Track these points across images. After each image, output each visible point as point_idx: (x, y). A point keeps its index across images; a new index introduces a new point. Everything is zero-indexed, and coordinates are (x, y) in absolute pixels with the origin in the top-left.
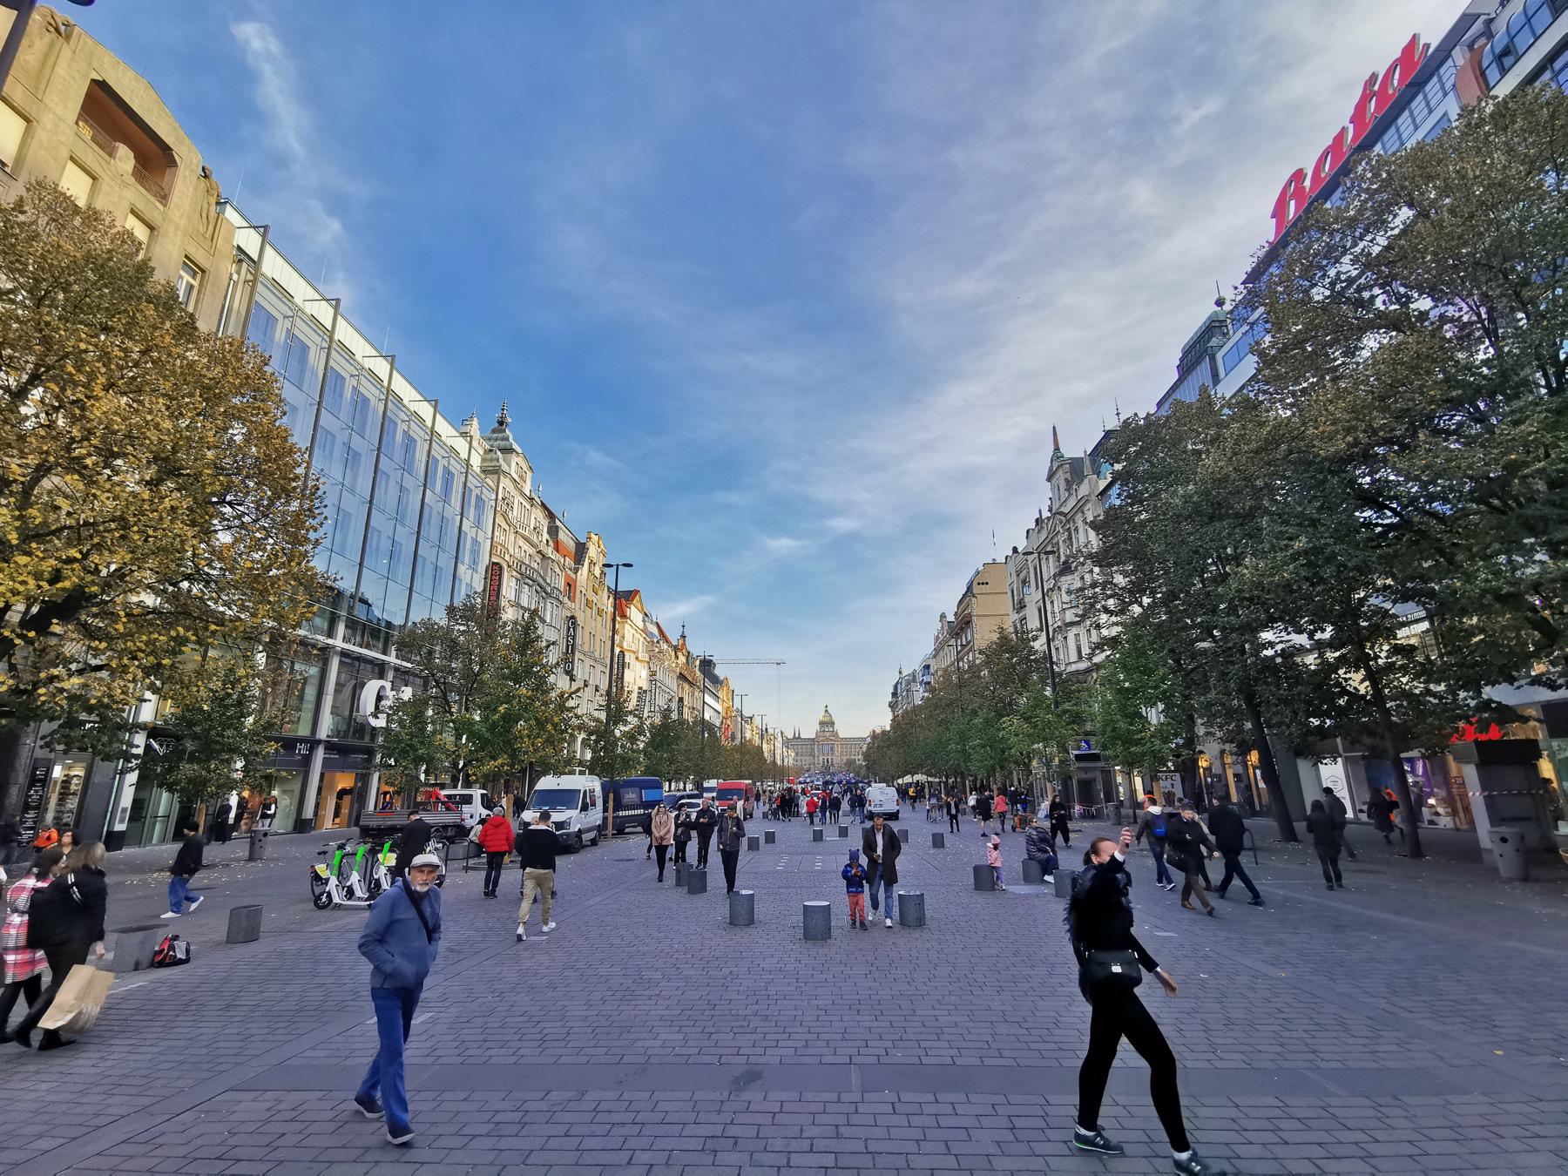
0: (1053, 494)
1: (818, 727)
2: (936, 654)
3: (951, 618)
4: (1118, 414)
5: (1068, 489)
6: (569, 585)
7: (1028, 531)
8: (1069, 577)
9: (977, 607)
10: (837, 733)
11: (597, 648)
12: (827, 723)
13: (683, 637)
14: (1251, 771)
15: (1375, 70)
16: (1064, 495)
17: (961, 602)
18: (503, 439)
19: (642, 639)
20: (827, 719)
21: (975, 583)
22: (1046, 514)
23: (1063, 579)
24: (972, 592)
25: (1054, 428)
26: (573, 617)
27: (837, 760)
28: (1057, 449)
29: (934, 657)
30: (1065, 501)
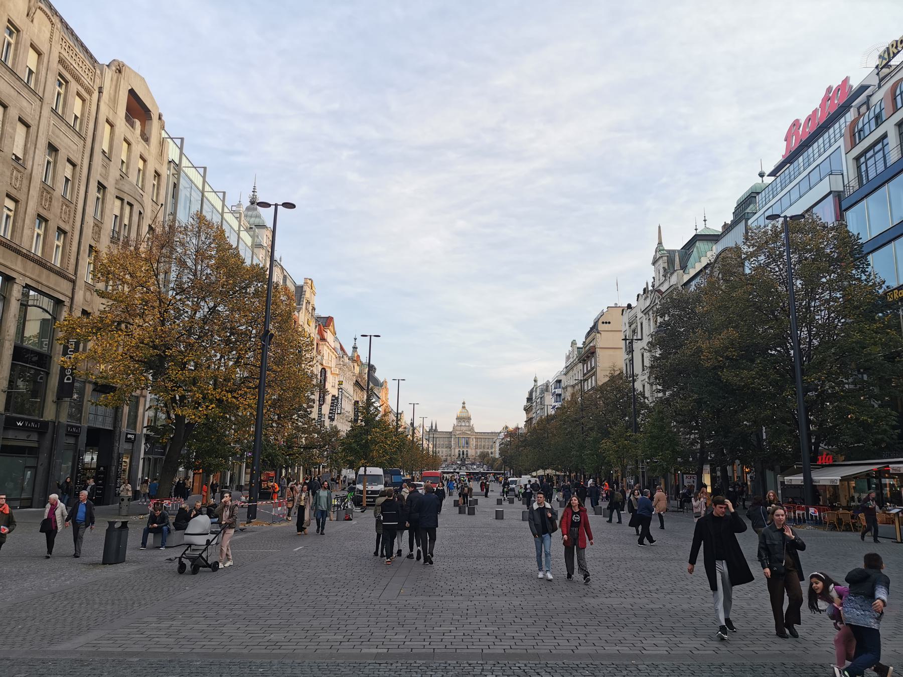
0: (656, 275)
1: (455, 422)
2: (569, 369)
3: (580, 345)
4: (705, 221)
5: (665, 276)
7: (638, 296)
9: (601, 341)
10: (472, 429)
12: (464, 419)
13: (355, 348)
14: (745, 475)
15: (831, 84)
16: (662, 279)
17: (589, 334)
18: (256, 217)
19: (334, 356)
20: (464, 415)
21: (600, 322)
22: (650, 288)
24: (597, 330)
25: (659, 227)
27: (471, 452)
28: (660, 243)
29: (565, 374)
30: (662, 283)
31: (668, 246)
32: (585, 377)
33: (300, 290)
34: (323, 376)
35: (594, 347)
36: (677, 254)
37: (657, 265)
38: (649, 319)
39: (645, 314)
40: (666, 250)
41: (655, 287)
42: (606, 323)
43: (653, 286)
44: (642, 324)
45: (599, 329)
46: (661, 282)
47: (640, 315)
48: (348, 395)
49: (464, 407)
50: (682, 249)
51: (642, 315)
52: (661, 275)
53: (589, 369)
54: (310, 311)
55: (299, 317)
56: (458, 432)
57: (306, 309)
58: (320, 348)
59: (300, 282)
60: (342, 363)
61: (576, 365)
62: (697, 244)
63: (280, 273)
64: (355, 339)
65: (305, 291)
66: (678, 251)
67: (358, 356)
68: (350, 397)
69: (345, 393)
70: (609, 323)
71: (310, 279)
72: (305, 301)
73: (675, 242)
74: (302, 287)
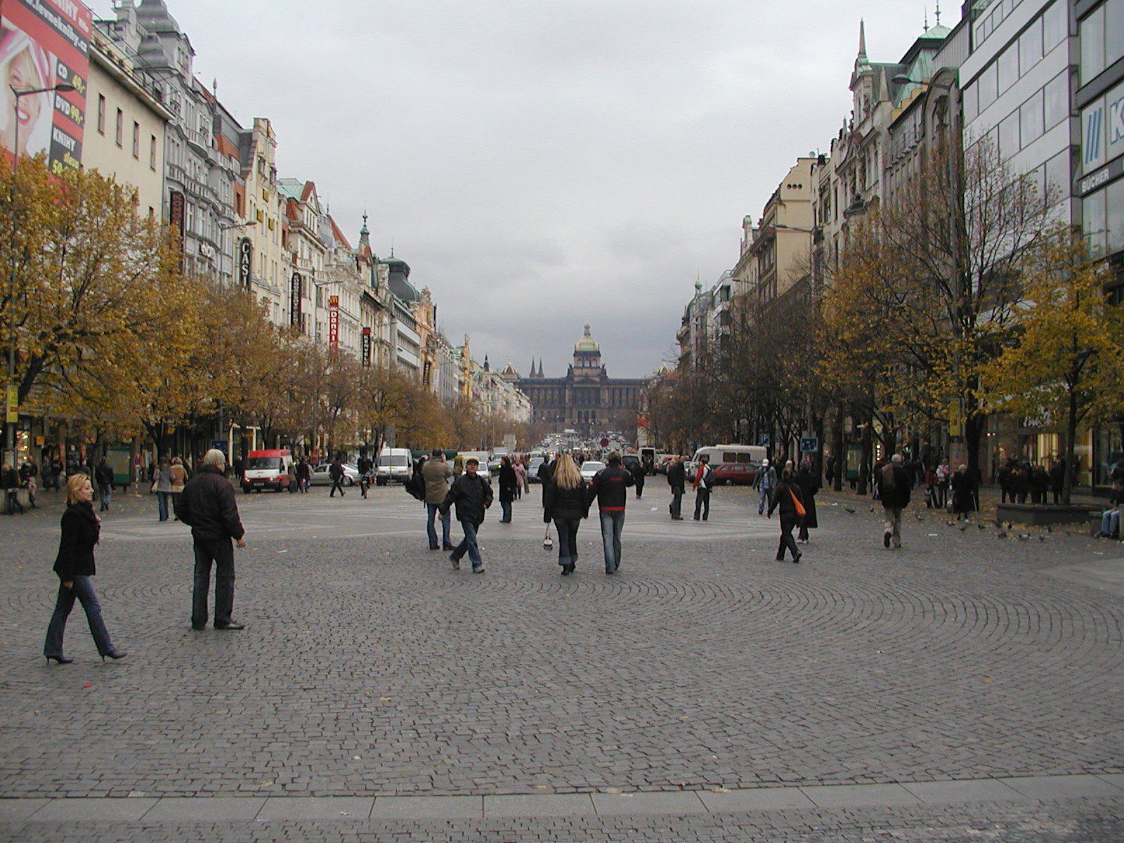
0: (855, 107)
2: (741, 266)
4: (938, 13)
6: (238, 196)
10: (604, 371)
11: (269, 274)
13: (365, 234)
16: (863, 115)
20: (589, 348)
21: (784, 188)
23: (852, 219)
24: (779, 199)
25: (862, 23)
26: (246, 240)
28: (862, 53)
30: (863, 122)
31: (873, 57)
33: (246, 141)
34: (296, 289)
36: (883, 73)
38: (846, 185)
39: (840, 175)
40: (871, 65)
41: (855, 128)
43: (851, 127)
45: (782, 198)
46: (863, 119)
47: (834, 177)
48: (349, 319)
49: (587, 334)
50: (901, 62)
52: (862, 108)
53: (767, 267)
54: (267, 175)
55: (245, 187)
56: (576, 379)
57: (259, 172)
58: (291, 238)
59: (247, 125)
60: (335, 263)
61: (749, 260)
62: (921, 55)
63: (207, 113)
64: (365, 218)
65: (256, 141)
67: (368, 249)
68: (354, 322)
69: (344, 315)
71: (263, 120)
72: (256, 159)
73: (889, 52)
74: (250, 135)
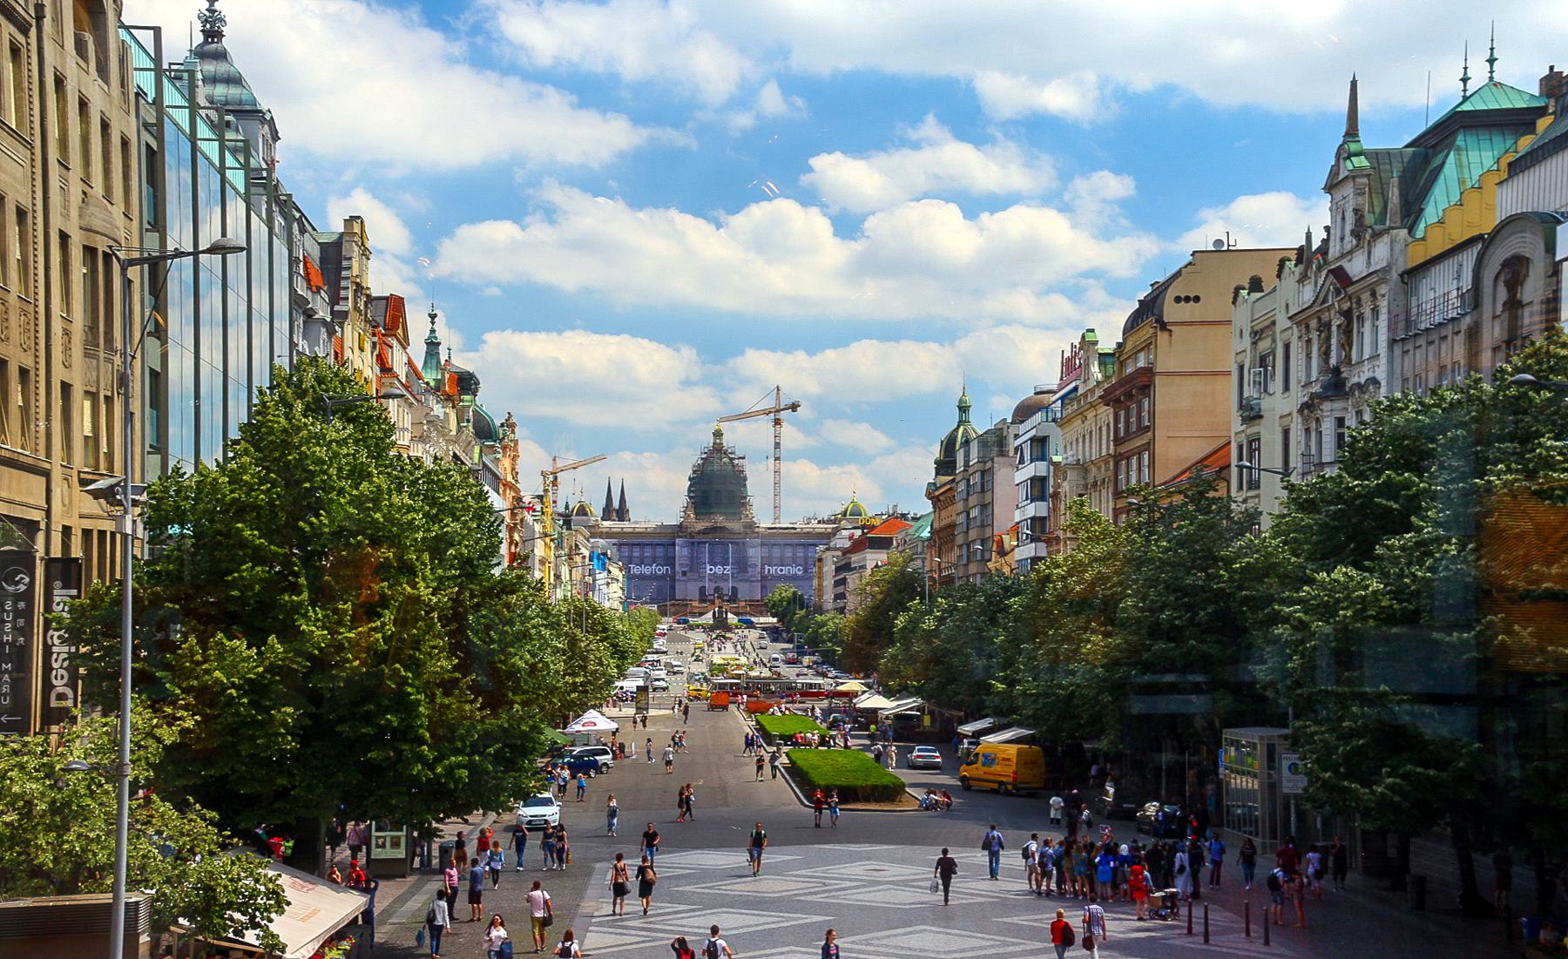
5: (1357, 234)
8: (1338, 405)
9: (1169, 355)
16: (1350, 241)
25: (1354, 84)
30: (1350, 252)
32: (1123, 449)
35: (1149, 372)
37: (1338, 195)
38: (1309, 341)
42: (1187, 299)
44: (1287, 346)
46: (1348, 247)
47: (1283, 322)
51: (1289, 324)
66: (1400, 153)
70: (1197, 299)
